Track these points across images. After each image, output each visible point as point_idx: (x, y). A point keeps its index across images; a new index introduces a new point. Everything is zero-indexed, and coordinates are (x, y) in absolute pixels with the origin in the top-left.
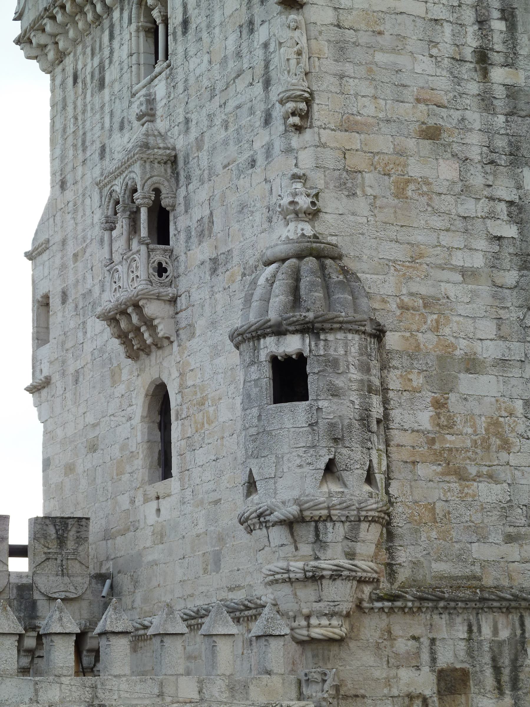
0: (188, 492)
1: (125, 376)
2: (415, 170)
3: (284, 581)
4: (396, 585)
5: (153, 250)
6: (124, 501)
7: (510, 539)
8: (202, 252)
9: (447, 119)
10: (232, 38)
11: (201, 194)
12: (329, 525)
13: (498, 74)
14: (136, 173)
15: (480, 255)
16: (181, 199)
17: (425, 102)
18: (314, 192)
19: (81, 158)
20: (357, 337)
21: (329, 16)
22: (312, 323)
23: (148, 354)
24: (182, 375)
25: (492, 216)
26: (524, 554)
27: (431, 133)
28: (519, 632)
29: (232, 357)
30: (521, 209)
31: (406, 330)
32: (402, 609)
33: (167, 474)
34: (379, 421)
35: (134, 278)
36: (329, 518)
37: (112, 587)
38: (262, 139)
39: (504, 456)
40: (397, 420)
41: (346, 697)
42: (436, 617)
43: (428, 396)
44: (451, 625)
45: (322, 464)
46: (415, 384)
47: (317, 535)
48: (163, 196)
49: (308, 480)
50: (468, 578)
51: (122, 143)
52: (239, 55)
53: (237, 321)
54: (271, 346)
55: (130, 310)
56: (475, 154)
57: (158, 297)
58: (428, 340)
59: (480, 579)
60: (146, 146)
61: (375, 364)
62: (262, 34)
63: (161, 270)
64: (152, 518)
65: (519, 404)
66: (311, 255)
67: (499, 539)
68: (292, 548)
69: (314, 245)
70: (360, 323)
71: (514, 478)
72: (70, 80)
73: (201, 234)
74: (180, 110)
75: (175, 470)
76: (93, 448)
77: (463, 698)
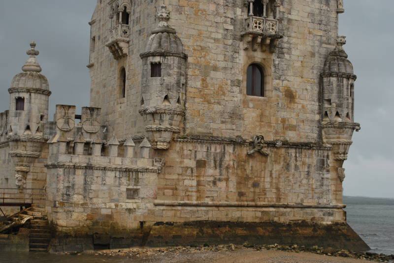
3: (150, 131)
4: (185, 135)
5: (123, 26)
6: (112, 103)
7: (223, 122)
11: (138, 10)
12: (165, 115)
18: (168, 12)
20: (177, 58)
23: (121, 59)
24: (129, 66)
25: (225, 22)
26: (227, 127)
28: (223, 150)
29: (141, 62)
30: (235, 21)
31: (195, 57)
32: (187, 141)
34: (183, 85)
36: (165, 112)
37: (107, 130)
39: (223, 97)
40: (190, 84)
42: (197, 144)
44: (202, 147)
46: (196, 73)
47: (161, 118)
48: (127, 9)
49: (159, 101)
50: (208, 133)
54: (151, 59)
55: (115, 44)
57: (123, 41)
63: (125, 32)
66: (166, 32)
67: (219, 122)
68: (153, 121)
69: (167, 29)
70: (179, 54)
71: (226, 104)
77: (204, 169)
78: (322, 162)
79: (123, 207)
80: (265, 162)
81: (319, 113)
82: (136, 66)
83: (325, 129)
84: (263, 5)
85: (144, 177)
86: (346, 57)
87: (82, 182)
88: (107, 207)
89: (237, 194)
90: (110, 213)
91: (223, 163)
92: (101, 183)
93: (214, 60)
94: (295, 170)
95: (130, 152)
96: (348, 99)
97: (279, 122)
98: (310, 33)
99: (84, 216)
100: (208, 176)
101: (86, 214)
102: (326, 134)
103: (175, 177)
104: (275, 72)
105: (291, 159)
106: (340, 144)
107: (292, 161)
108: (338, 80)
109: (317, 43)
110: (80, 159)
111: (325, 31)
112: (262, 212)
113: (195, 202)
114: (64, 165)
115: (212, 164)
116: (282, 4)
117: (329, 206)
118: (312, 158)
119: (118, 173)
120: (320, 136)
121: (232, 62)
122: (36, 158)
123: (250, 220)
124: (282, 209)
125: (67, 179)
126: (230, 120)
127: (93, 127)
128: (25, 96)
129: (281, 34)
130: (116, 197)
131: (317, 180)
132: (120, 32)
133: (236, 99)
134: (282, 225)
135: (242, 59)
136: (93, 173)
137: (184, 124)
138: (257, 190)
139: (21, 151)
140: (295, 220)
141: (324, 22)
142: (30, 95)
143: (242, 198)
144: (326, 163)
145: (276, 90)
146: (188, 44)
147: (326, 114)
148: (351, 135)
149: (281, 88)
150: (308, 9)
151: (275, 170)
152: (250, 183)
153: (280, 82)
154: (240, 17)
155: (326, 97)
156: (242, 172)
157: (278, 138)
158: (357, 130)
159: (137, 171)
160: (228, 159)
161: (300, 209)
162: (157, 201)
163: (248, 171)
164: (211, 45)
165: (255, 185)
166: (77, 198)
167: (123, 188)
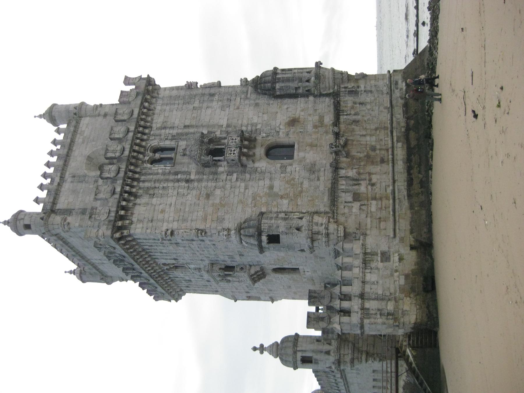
2: (217, 201)
6: (304, 280)
7: (318, 179)
8: (237, 258)
9: (204, 192)
10: (180, 248)
11: (222, 258)
13: (193, 177)
14: (215, 274)
15: (241, 184)
16: (223, 263)
21: (175, 223)
22: (258, 233)
25: (231, 180)
27: (208, 196)
29: (267, 253)
34: (286, 215)
35: (244, 276)
36: (311, 230)
37: (328, 284)
39: (296, 180)
41: (360, 227)
43: (279, 200)
44: (341, 197)
50: (329, 191)
51: (206, 276)
52: (185, 247)
53: (256, 251)
56: (214, 184)
57: (249, 270)
58: (264, 200)
60: (208, 271)
61: (270, 215)
62: (179, 241)
63: (242, 269)
64: (310, 273)
65: (282, 175)
67: (318, 182)
68: (319, 241)
70: (259, 219)
72: (188, 288)
73: (233, 258)
79: (397, 265)
80: (353, 141)
81: (307, 96)
82: (272, 257)
83: (322, 91)
85: (369, 247)
86: (258, 77)
87: (376, 301)
89: (383, 165)
90: (403, 277)
91: (355, 178)
93: (264, 189)
95: (347, 260)
96: (295, 73)
97: (317, 130)
98: (238, 108)
99: (407, 301)
101: (405, 298)
103: (369, 220)
106: (334, 78)
108: (278, 82)
109: (247, 102)
112: (398, 141)
113: (391, 201)
114: (361, 318)
115: (356, 187)
116: (215, 132)
117: (389, 85)
118: (347, 101)
119: (367, 271)
120: (327, 95)
121: (265, 173)
122: (354, 346)
123: (405, 152)
124: (394, 125)
128: (299, 355)
129: (240, 132)
131: (367, 96)
132: (242, 274)
133: (297, 169)
134: (408, 124)
135: (263, 164)
137: (321, 213)
138: (378, 147)
139: (348, 358)
140: (403, 112)
141: (229, 97)
142: (299, 351)
143: (386, 160)
144: (351, 89)
145: (288, 135)
146: (250, 212)
149: (287, 130)
150: (218, 111)
151: (359, 133)
152: (372, 153)
153: (281, 131)
154: (226, 168)
157: (331, 130)
158: (321, 64)
159: (365, 254)
160: (352, 173)
162: (392, 236)
164: (250, 192)
165: (374, 149)
166: (390, 306)
167: (380, 265)
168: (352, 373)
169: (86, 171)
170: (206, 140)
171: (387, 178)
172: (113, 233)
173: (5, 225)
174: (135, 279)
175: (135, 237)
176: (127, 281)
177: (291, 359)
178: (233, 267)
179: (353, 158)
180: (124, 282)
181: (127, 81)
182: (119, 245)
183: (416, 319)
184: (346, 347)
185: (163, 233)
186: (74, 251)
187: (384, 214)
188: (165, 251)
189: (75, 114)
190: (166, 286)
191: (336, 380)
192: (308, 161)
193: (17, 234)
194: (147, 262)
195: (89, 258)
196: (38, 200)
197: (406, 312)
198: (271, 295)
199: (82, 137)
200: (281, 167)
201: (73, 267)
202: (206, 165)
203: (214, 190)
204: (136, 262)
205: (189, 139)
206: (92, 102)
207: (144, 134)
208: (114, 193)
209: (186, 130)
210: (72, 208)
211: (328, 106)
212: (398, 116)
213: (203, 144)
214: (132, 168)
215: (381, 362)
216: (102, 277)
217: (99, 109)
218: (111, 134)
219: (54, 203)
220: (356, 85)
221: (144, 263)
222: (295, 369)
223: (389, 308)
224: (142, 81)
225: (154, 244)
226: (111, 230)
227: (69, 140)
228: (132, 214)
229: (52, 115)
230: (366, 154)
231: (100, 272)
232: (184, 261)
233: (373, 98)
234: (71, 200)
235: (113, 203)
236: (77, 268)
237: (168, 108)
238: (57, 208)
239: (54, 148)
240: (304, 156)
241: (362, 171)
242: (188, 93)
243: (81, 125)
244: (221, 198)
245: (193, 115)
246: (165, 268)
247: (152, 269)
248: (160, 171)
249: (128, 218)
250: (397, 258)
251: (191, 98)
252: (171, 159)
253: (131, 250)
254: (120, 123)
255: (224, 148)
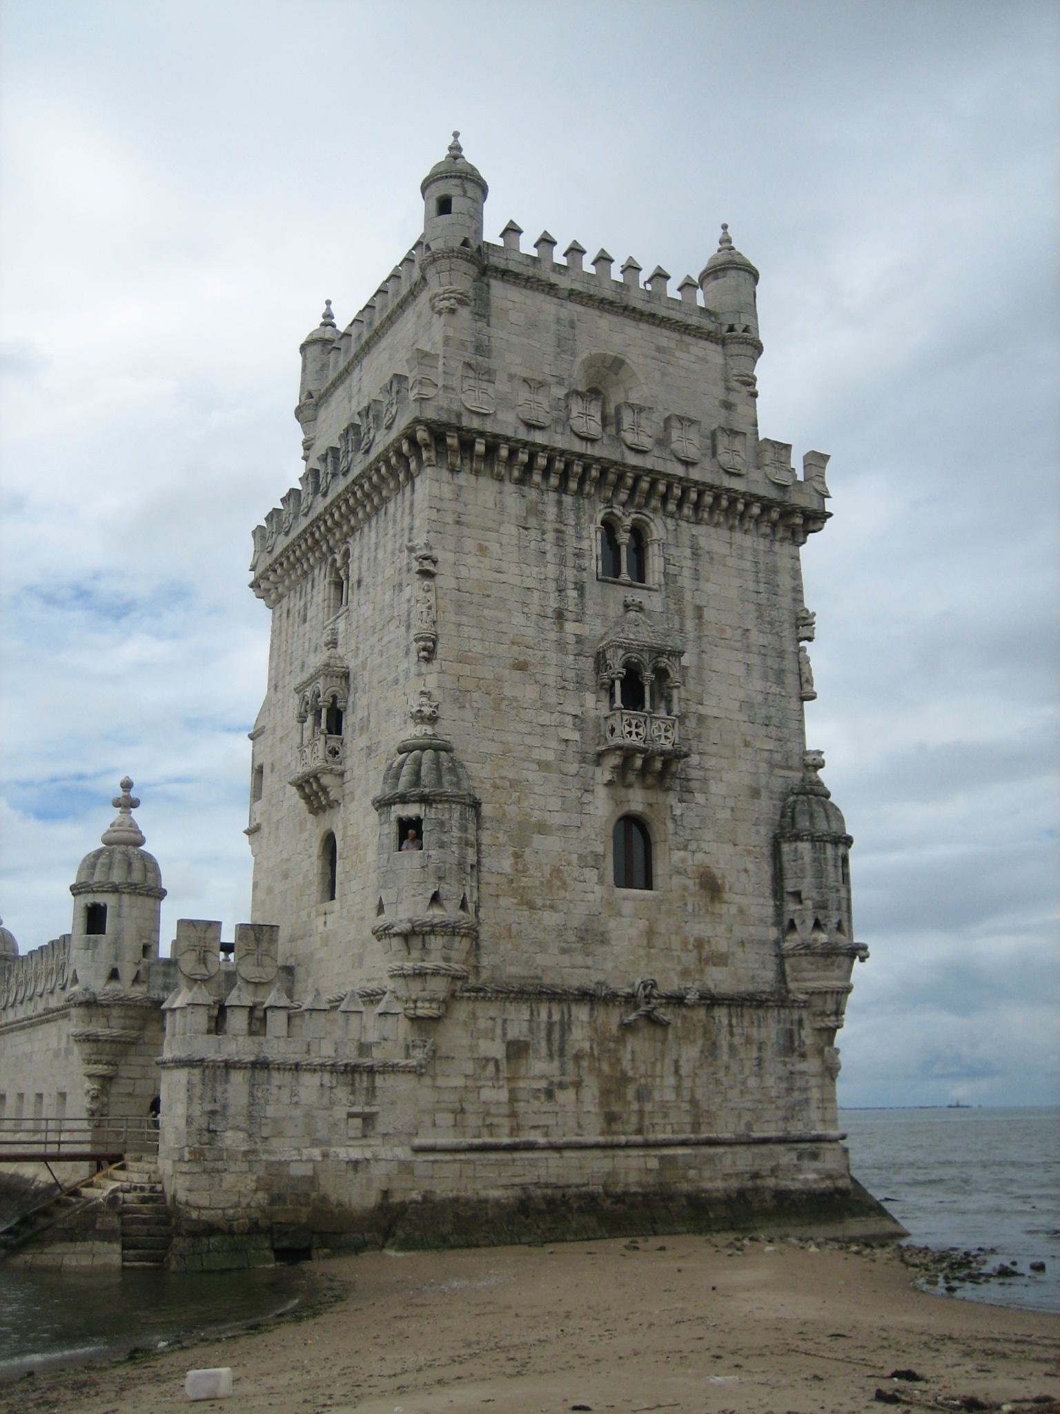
0: (345, 911)
1: (308, 826)
2: (508, 691)
3: (400, 976)
4: (481, 981)
6: (304, 914)
7: (564, 951)
10: (389, 593)
12: (432, 937)
13: (570, 627)
16: (350, 703)
17: (518, 644)
19: (288, 669)
20: (459, 807)
21: (453, 583)
24: (345, 827)
25: (562, 725)
27: (521, 666)
28: (566, 1016)
29: (374, 817)
30: (583, 721)
32: (483, 998)
33: (333, 898)
34: (472, 866)
35: (316, 759)
38: (404, 664)
39: (562, 893)
41: (440, 1058)
45: (430, 895)
46: (501, 840)
47: (424, 945)
50: (532, 978)
51: (316, 661)
53: (378, 791)
56: (551, 681)
58: (512, 810)
59: (540, 979)
60: (328, 665)
61: (472, 826)
63: (334, 753)
64: (321, 928)
67: (556, 951)
70: (462, 797)
72: (285, 615)
73: (362, 729)
74: (353, 641)
75: (337, 895)
76: (285, 876)
78: (790, 1035)
80: (664, 1041)
81: (778, 923)
82: (363, 828)
84: (642, 687)
86: (828, 795)
87: (245, 1100)
88: (304, 1158)
90: (310, 1173)
91: (567, 1047)
92: (287, 1101)
94: (730, 1057)
96: (838, 890)
97: (690, 947)
98: (747, 744)
99: (250, 1182)
100: (534, 1078)
101: (254, 1178)
102: (794, 970)
103: (459, 1082)
104: (676, 833)
105: (719, 1030)
106: (826, 992)
107: (722, 1036)
108: (814, 847)
109: (764, 767)
110: (237, 1044)
111: (780, 740)
112: (662, 1159)
113: (506, 1140)
114: (202, 1060)
118: (770, 1029)
119: (327, 1076)
120: (782, 975)
122: (129, 1043)
125: (209, 1094)
126: (580, 945)
127: (260, 969)
129: (685, 749)
130: (322, 1133)
131: (780, 1078)
135: (602, 809)
136: (269, 1076)
138: (648, 1107)
139: (98, 1028)
141: (775, 721)
143: (614, 1127)
144: (796, 1037)
145: (679, 873)
146: (480, 775)
147: (792, 926)
148: (850, 971)
150: (741, 694)
151: (684, 1057)
152: (630, 1092)
154: (593, 714)
155: (790, 885)
156: (612, 1066)
158: (862, 960)
159: (371, 1071)
160: (579, 1037)
161: (744, 1148)
162: (418, 1141)
163: (624, 1063)
164: (533, 776)
165: (641, 1096)
166: (233, 1139)
167: (340, 1112)
168: (60, 1039)
169: (584, 355)
170: (664, 661)
171: (567, 1134)
172: (430, 426)
173: (451, 148)
174: (310, 479)
175: (418, 481)
176: (306, 458)
177: (98, 877)
178: (339, 732)
179: (620, 1040)
180: (301, 452)
181: (817, 461)
182: (398, 440)
183: (199, 1208)
184: (128, 1022)
185: (424, 552)
186: (382, 325)
187: (473, 1121)
188: (380, 555)
189: (731, 329)
190: (292, 558)
191: (41, 996)
192: (612, 924)
193: (427, 179)
194: (353, 511)
195: (365, 362)
196: (512, 234)
197: (217, 1179)
198: (265, 830)
199: (673, 345)
200: (596, 855)
201: (342, 323)
202: (600, 661)
203: (537, 682)
204: (354, 482)
205: (668, 619)
206: (763, 370)
207: (680, 504)
208: (530, 426)
209: (689, 612)
210: (493, 320)
211: (753, 978)
212: (727, 1161)
213: (655, 655)
214: (594, 473)
215: (85, 1115)
216: (316, 395)
217: (744, 389)
218: (681, 419)
219: (505, 274)
220: (808, 1048)
221: (351, 501)
222: (72, 888)
223: (229, 1133)
224: (816, 497)
225: (398, 528)
226: (436, 418)
227: (663, 312)
228: (477, 473)
229: (731, 268)
230: (630, 1074)
231: (328, 390)
232: (355, 603)
233: (773, 1093)
234: (513, 316)
235: (507, 424)
236: (338, 332)
237: (748, 565)
238: (493, 282)
239: (644, 276)
240: (624, 912)
241: (585, 1064)
242: (786, 616)
243: (702, 343)
244: (515, 699)
245: (729, 630)
246: (338, 557)
247: (337, 524)
248: (585, 545)
249: (467, 461)
250: (356, 1154)
251: (771, 623)
252: (617, 573)
253: (383, 470)
254: (708, 442)
255: (643, 707)
